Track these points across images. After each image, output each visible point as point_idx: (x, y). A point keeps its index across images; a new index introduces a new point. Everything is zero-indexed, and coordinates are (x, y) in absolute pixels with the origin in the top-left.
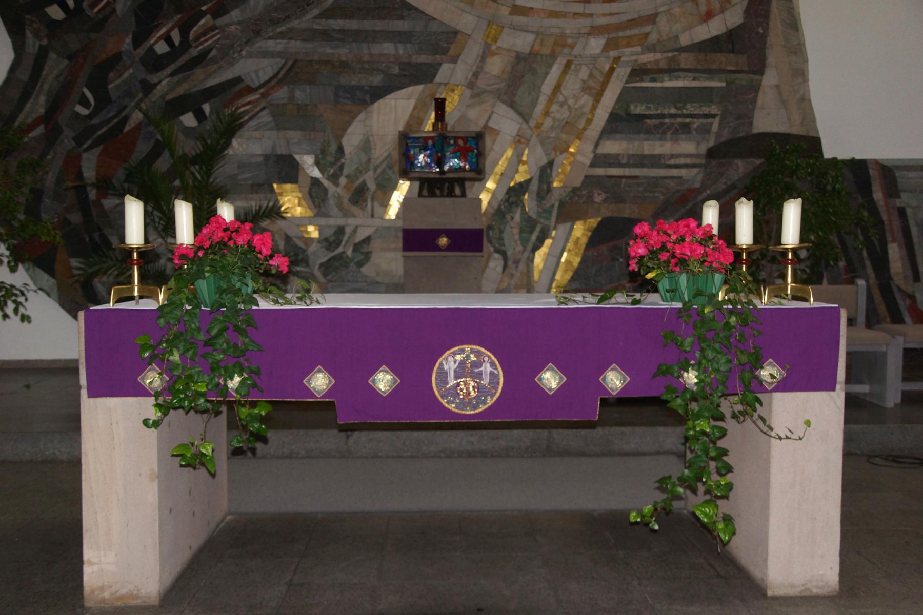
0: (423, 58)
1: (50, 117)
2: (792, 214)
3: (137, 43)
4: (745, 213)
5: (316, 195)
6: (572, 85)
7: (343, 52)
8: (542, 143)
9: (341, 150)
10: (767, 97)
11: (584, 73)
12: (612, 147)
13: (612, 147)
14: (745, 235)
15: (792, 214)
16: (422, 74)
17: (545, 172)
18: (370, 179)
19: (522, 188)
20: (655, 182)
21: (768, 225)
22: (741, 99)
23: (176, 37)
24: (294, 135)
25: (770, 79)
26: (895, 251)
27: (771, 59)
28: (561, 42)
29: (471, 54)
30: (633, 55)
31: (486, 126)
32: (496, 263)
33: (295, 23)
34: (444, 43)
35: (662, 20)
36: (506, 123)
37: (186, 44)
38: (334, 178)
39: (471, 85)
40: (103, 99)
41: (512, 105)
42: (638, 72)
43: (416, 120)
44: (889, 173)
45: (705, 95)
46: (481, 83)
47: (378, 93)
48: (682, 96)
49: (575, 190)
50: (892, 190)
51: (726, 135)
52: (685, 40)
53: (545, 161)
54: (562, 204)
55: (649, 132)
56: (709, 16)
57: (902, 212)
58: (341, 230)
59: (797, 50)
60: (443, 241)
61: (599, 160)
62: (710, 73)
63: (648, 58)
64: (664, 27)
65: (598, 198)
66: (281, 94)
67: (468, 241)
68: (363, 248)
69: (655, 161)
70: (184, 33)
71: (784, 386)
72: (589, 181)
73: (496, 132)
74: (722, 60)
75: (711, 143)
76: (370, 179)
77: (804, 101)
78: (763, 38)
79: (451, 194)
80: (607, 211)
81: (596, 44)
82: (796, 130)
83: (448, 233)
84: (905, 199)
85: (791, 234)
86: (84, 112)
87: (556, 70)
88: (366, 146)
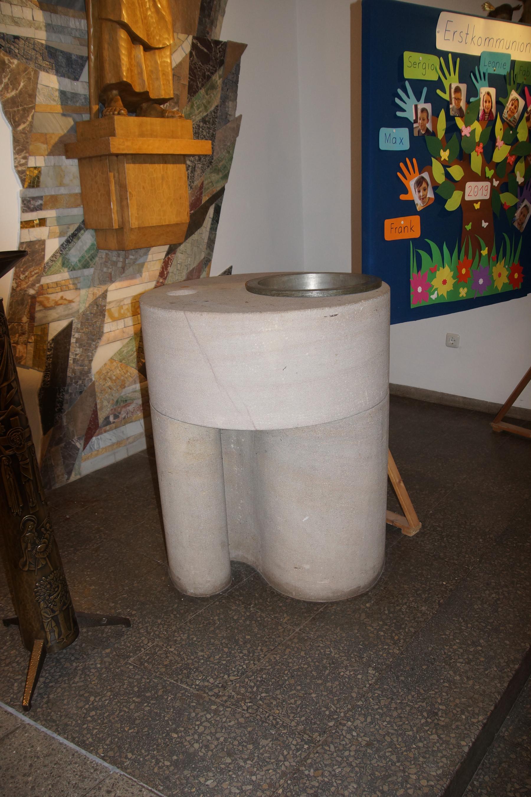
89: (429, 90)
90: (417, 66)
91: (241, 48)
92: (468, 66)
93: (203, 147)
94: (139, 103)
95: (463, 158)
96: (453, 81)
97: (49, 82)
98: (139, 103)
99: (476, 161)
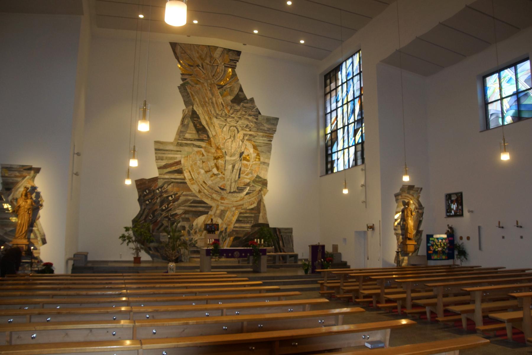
0: (207, 210)
1: (145, 219)
2: (262, 240)
3: (160, 207)
4: (259, 240)
5: (189, 232)
7: (194, 209)
8: (226, 224)
9: (193, 225)
10: (261, 217)
12: (237, 225)
13: (237, 225)
14: (259, 242)
15: (262, 240)
16: (207, 213)
17: (226, 229)
18: (197, 230)
20: (244, 231)
21: (260, 241)
22: (257, 218)
23: (166, 206)
24: (185, 223)
25: (261, 215)
26: (281, 242)
28: (228, 208)
33: (186, 204)
34: (210, 207)
37: (168, 207)
38: (192, 230)
40: (154, 216)
41: (221, 218)
42: (241, 213)
45: (251, 217)
46: (216, 214)
47: (199, 216)
48: (247, 217)
50: (280, 233)
52: (248, 208)
56: (251, 204)
57: (281, 236)
58: (192, 239)
59: (265, 210)
61: (234, 227)
62: (252, 213)
63: (242, 211)
64: (245, 206)
65: (234, 233)
66: (183, 216)
68: (196, 242)
69: (243, 228)
70: (168, 205)
72: (233, 231)
74: (253, 212)
75: (252, 224)
76: (197, 230)
77: (266, 218)
80: (236, 236)
81: (234, 209)
82: (265, 223)
84: (282, 234)
85: (262, 242)
86: (150, 218)
88: (197, 225)
89: (433, 241)
90: (431, 239)
91: (422, 231)
92: (437, 239)
93: (416, 243)
94: (410, 239)
96: (436, 240)
97: (401, 237)
98: (410, 239)
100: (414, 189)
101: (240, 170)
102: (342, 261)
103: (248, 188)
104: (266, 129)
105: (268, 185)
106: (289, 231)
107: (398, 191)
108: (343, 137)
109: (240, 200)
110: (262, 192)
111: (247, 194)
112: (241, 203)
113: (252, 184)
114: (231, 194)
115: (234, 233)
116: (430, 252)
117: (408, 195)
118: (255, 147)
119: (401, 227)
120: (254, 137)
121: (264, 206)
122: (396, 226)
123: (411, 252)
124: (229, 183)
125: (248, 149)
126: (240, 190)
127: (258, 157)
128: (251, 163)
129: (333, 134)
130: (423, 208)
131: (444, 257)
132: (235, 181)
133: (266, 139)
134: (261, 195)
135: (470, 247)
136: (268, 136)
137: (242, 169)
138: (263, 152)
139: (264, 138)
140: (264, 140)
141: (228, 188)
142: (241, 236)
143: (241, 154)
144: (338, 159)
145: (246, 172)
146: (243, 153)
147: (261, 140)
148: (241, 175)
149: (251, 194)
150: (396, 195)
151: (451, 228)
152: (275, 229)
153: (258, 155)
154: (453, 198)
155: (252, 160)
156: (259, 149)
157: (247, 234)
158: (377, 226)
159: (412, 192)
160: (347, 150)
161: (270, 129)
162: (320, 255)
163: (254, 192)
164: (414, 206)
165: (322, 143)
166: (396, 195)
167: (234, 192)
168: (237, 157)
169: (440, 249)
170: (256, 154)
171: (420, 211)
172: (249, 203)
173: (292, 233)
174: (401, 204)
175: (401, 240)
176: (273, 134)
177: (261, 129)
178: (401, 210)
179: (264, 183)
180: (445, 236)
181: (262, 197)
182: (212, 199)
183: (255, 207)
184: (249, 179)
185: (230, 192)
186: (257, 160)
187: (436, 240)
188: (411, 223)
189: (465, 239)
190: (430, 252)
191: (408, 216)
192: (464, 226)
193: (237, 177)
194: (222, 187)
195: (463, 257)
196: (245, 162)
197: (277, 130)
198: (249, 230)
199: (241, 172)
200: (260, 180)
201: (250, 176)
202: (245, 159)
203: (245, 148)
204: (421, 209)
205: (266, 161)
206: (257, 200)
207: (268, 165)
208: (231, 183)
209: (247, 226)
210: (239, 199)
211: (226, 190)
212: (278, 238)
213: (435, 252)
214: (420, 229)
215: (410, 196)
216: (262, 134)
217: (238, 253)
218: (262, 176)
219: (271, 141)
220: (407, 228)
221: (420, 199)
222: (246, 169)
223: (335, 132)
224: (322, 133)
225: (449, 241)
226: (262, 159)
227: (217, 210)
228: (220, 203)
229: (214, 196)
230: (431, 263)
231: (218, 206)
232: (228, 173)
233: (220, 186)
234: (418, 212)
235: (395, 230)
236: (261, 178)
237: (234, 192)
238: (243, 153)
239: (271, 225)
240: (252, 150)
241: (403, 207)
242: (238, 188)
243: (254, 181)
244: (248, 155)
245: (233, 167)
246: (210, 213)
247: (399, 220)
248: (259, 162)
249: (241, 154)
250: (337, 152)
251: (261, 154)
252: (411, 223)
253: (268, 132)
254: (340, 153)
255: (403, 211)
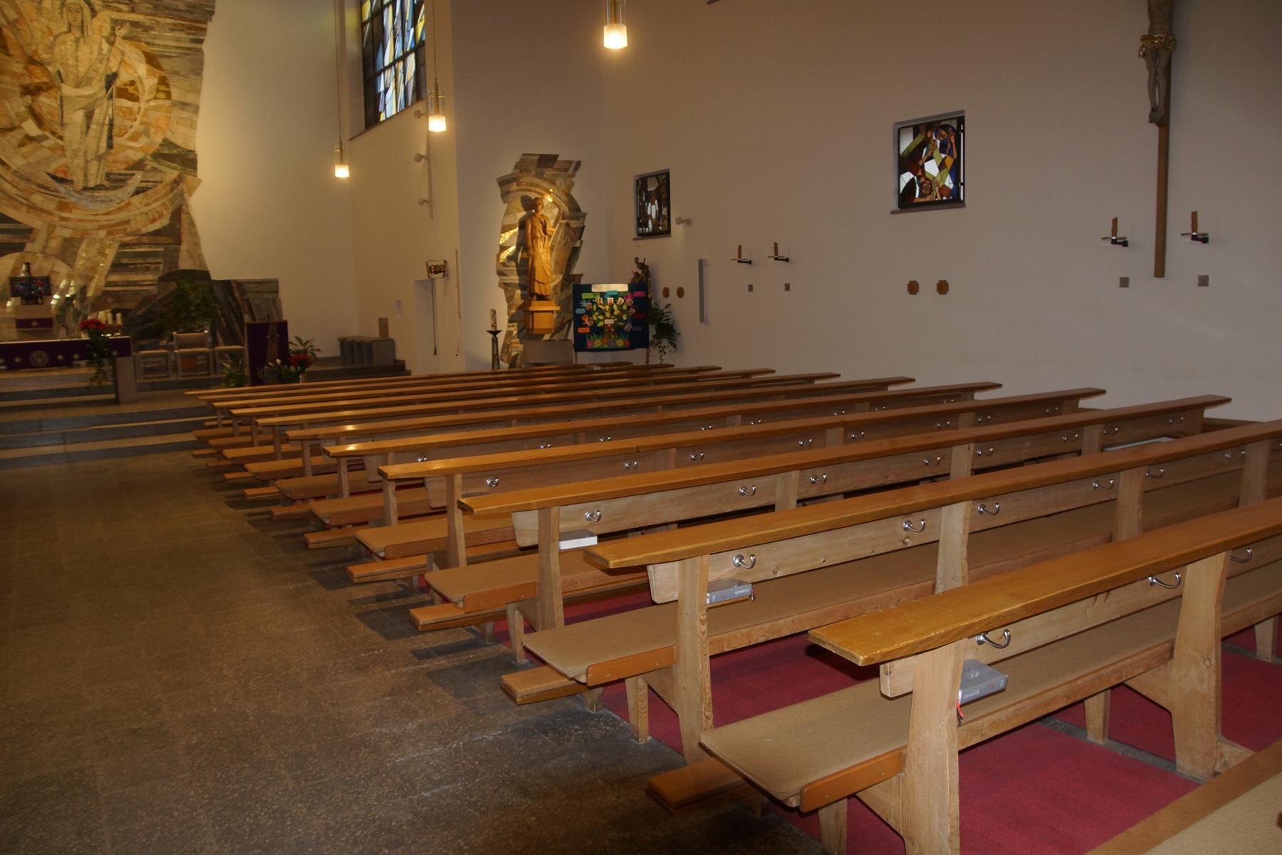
0: (17, 241)
6: (93, 251)
11: (98, 246)
14: (110, 322)
15: (119, 315)
16: (19, 248)
17: (83, 290)
19: (73, 297)
22: (171, 256)
25: (184, 247)
27: (184, 237)
28: (85, 233)
29: (41, 238)
30: (121, 238)
31: (52, 271)
32: (63, 332)
35: (132, 223)
36: (62, 268)
39: (43, 253)
41: (64, 261)
42: (124, 245)
43: (16, 269)
44: (240, 284)
45: (155, 254)
46: (48, 251)
49: (98, 298)
50: (243, 292)
51: (167, 271)
52: (144, 231)
53: (81, 283)
54: (93, 305)
55: (131, 271)
56: (154, 220)
57: (248, 301)
59: (195, 234)
60: (34, 323)
61: (108, 284)
62: (157, 245)
63: (128, 239)
64: (134, 226)
65: (110, 300)
67: (46, 323)
69: (135, 284)
71: (120, 355)
72: (105, 293)
73: (57, 273)
74: (161, 239)
77: (200, 255)
78: (179, 230)
79: (37, 303)
80: (115, 306)
81: (102, 233)
83: (38, 320)
84: (249, 296)
87: (84, 245)
89: (591, 300)
90: (585, 296)
91: (581, 275)
92: (602, 295)
93: (558, 308)
94: (542, 298)
95: (603, 314)
96: (598, 298)
97: (519, 292)
98: (542, 298)
99: (608, 315)
100: (556, 166)
101: (111, 125)
102: (395, 361)
103: (139, 175)
104: (182, 7)
105: (200, 165)
106: (270, 287)
107: (508, 170)
108: (394, 28)
109: (120, 209)
110: (182, 186)
111: (137, 192)
112: (122, 216)
113: (150, 164)
114: (88, 193)
115: (110, 300)
116: (581, 330)
117: (538, 181)
118: (152, 60)
119: (517, 266)
120: (147, 29)
121: (192, 224)
122: (504, 264)
123: (548, 331)
124: (80, 161)
125: (130, 66)
126: (116, 181)
127: (163, 88)
128: (143, 105)
129: (376, 21)
130: (584, 215)
131: (620, 343)
132: (99, 158)
133: (183, 35)
134: (182, 194)
135: (683, 312)
136: (190, 28)
137: (117, 122)
138: (177, 73)
139: (178, 34)
140: (178, 40)
141: (78, 177)
142: (130, 305)
143: (111, 79)
144: (386, 90)
145: (131, 131)
146: (115, 75)
147: (168, 38)
148: (116, 140)
149: (150, 192)
150: (504, 182)
151: (642, 266)
152: (227, 284)
153: (163, 81)
154: (651, 188)
155: (144, 97)
156: (165, 63)
157: (148, 299)
158: (452, 267)
159: (549, 173)
160: (400, 65)
161: (194, 7)
162: (273, 348)
163: (160, 186)
164: (556, 211)
165: (353, 47)
166: (504, 182)
167: (99, 188)
168: (96, 88)
169: (609, 322)
170: (156, 81)
171: (574, 224)
172: (145, 215)
173: (277, 292)
174: (519, 204)
175: (518, 300)
176: (205, 22)
177: (166, 8)
178: (517, 222)
179: (187, 161)
180: (623, 288)
181: (184, 200)
182: (33, 207)
183: (164, 228)
184: (141, 149)
185: (85, 189)
186: (163, 96)
187: (598, 299)
188: (545, 256)
189: (673, 293)
190: (581, 330)
191: (534, 237)
192: (671, 259)
193: (104, 144)
194: (60, 175)
195: (665, 342)
196: (125, 103)
197: (217, 11)
198: (153, 289)
199: (115, 130)
200: (175, 152)
201: (143, 141)
202: (123, 93)
203: (122, 62)
204: (576, 218)
205: (189, 98)
206: (171, 208)
207: (196, 109)
208: (87, 162)
209: (147, 279)
210: (114, 206)
211: (71, 182)
212: (238, 306)
213: (597, 331)
214: (575, 271)
215: (545, 185)
216: (169, 21)
217: (44, 355)
218: (179, 141)
219: (201, 42)
220: (533, 269)
221: (574, 193)
222: (129, 123)
223: (378, 14)
224: (351, 20)
225: (635, 299)
226: (176, 94)
227: (48, 238)
228: (56, 219)
229: (37, 199)
230: (583, 358)
231: (51, 228)
232: (73, 134)
233: (51, 170)
234: (568, 225)
235: (500, 273)
236: (176, 147)
237: (99, 188)
238: (115, 75)
239: (214, 277)
240: (142, 69)
241: (524, 213)
242: (108, 175)
243: (157, 156)
244: (132, 83)
245: (89, 116)
246: (29, 247)
247: (513, 248)
248: (168, 103)
249: (111, 79)
250: (385, 69)
251: (172, 80)
252: (545, 256)
253: (190, 16)
254: (390, 74)
255: (522, 225)
